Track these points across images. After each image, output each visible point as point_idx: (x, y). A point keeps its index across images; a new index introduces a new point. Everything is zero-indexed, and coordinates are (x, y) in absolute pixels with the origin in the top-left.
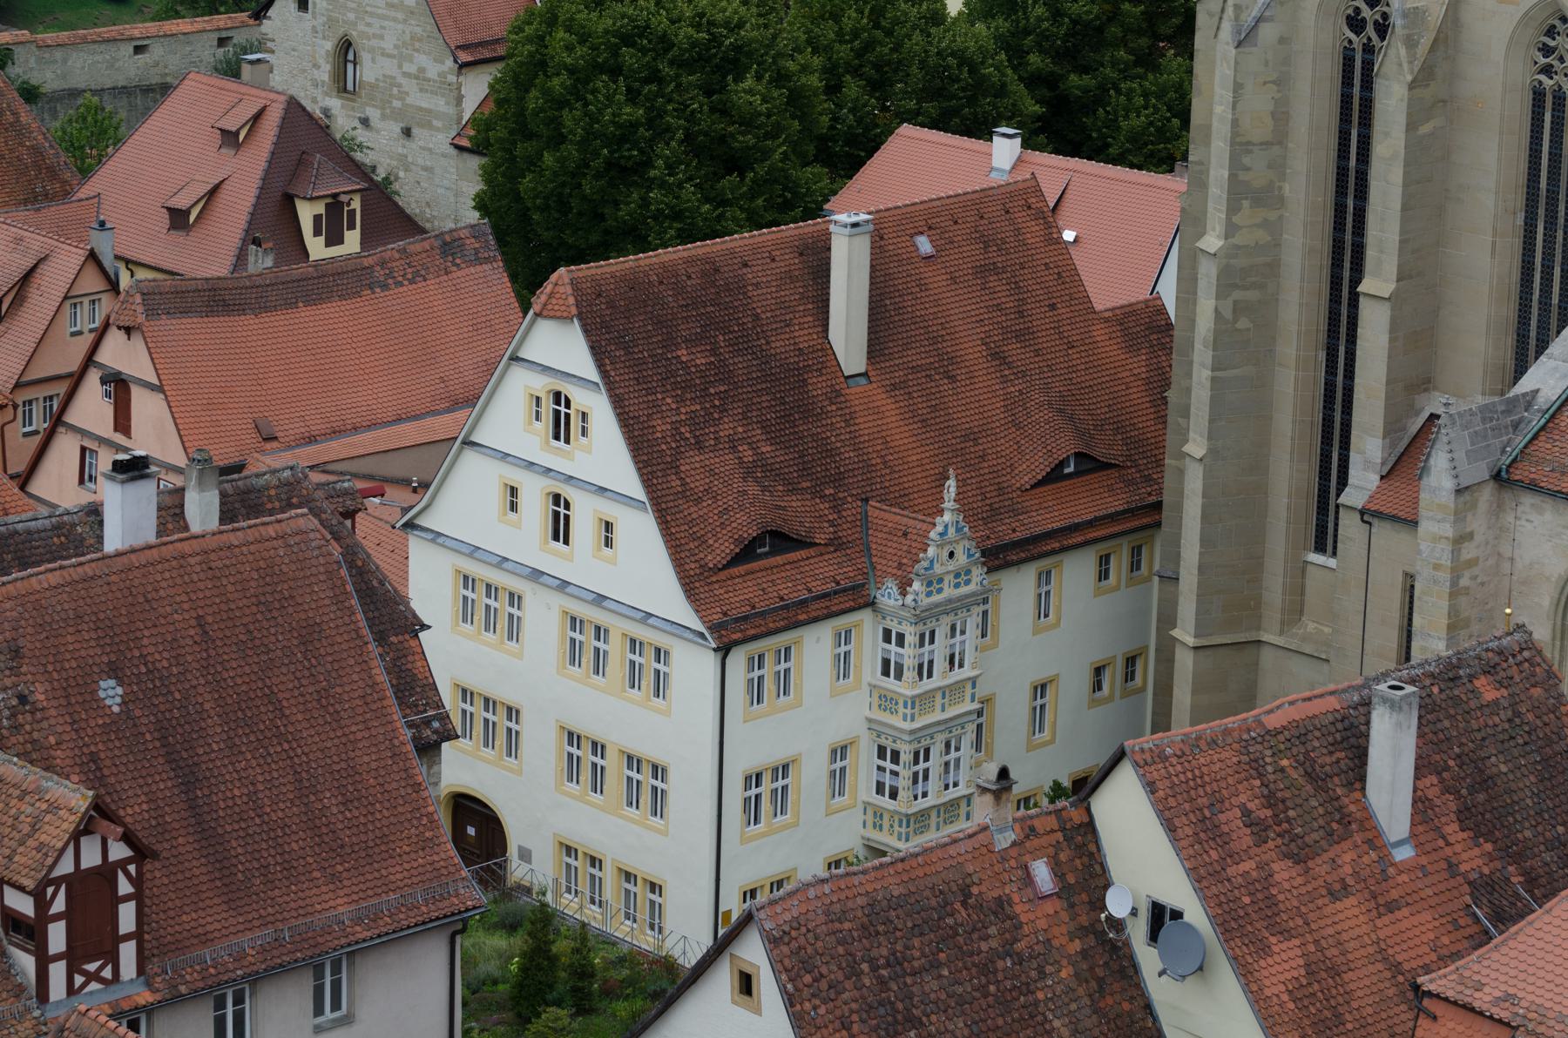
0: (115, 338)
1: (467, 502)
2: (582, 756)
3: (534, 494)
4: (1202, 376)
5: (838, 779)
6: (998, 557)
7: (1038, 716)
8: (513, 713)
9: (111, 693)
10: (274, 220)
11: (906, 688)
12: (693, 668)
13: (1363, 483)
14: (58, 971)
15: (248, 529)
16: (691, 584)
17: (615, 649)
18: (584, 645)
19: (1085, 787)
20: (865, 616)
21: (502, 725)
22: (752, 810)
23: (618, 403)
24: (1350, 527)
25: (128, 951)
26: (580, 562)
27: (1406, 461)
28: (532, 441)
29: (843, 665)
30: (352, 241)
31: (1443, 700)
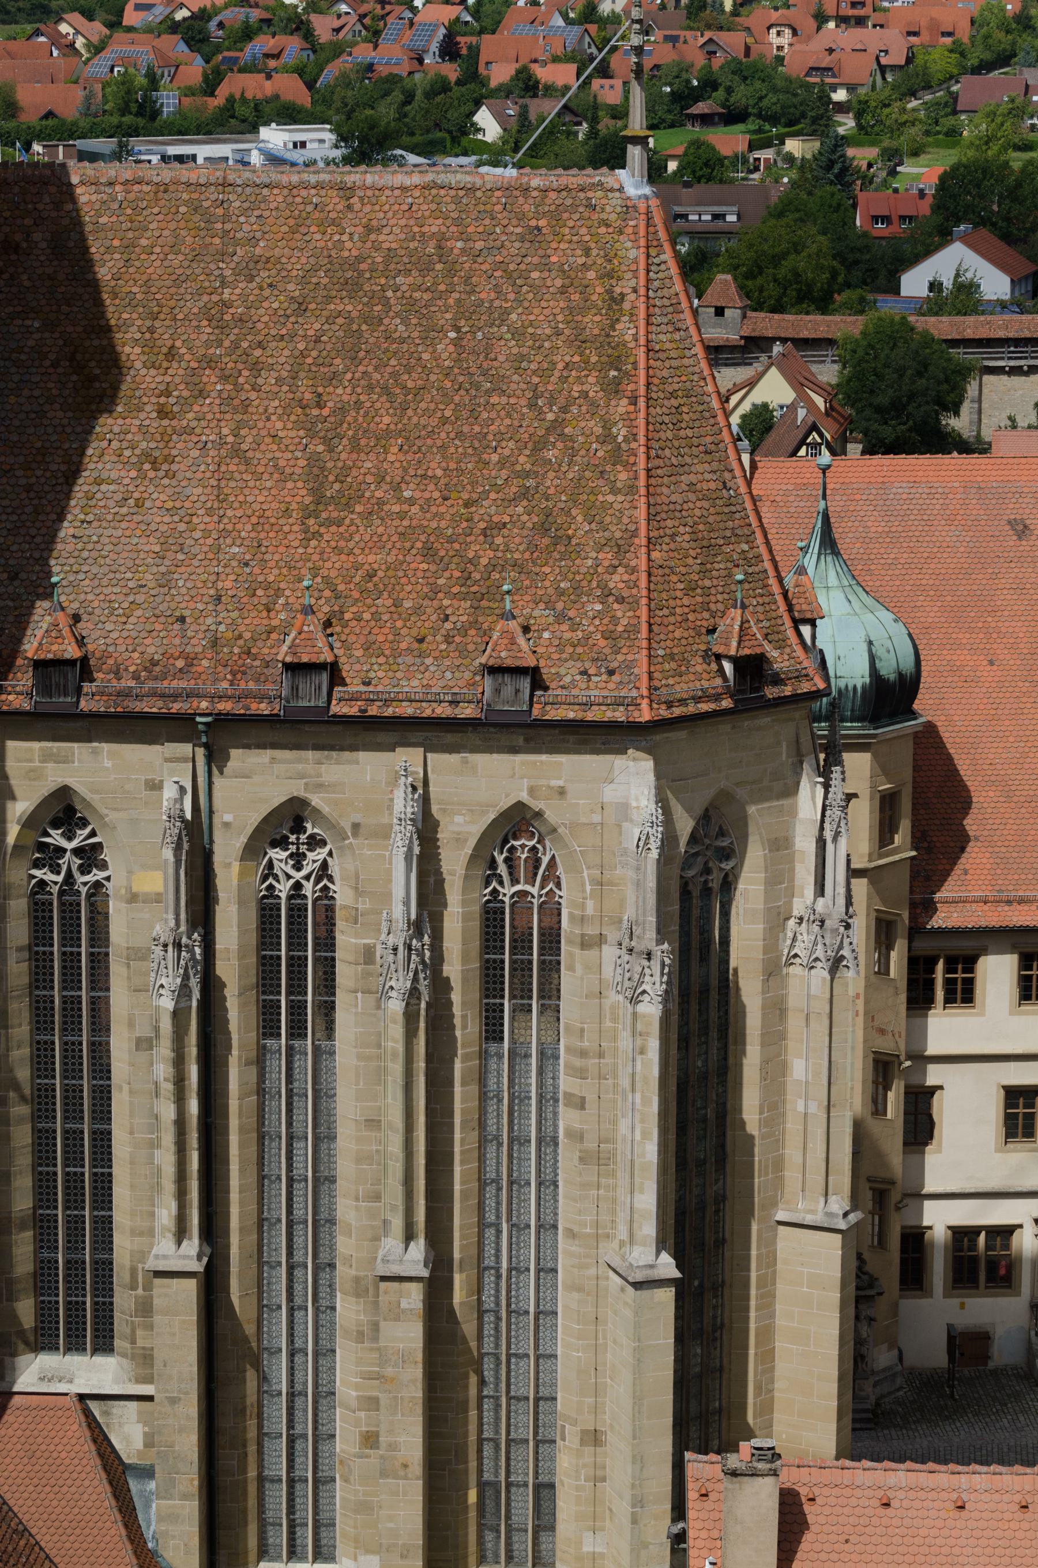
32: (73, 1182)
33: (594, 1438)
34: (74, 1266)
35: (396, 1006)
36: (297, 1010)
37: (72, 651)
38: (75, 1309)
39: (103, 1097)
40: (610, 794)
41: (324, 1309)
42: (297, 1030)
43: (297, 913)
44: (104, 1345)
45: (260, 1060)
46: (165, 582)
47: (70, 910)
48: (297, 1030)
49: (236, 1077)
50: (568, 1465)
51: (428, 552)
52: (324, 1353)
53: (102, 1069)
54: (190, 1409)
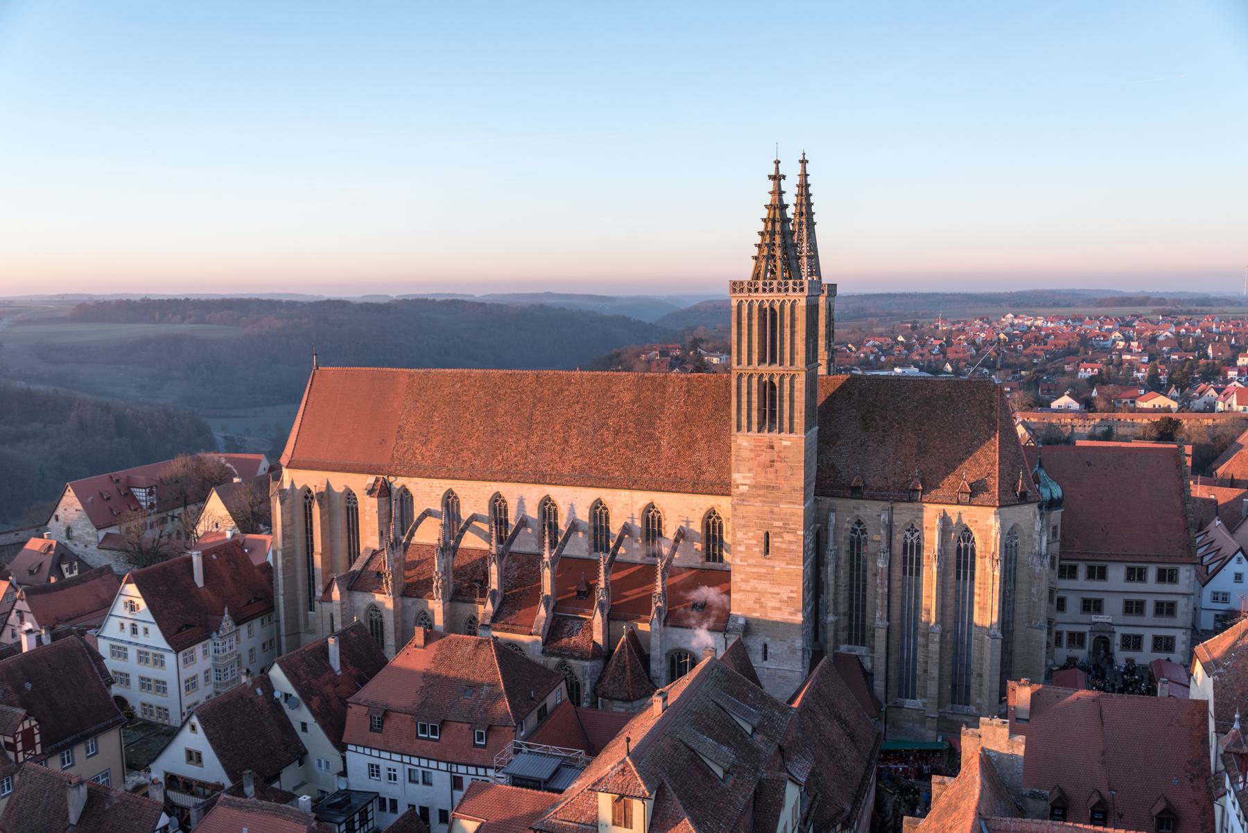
0: (19, 602)
1: (112, 628)
2: (145, 683)
3: (127, 624)
4: (280, 576)
5: (207, 679)
6: (238, 623)
7: (251, 657)
8: (127, 675)
9: (28, 686)
10: (56, 568)
11: (221, 655)
12: (170, 658)
13: (319, 594)
14: (20, 755)
15: (59, 642)
16: (168, 639)
17: (150, 656)
18: (143, 658)
19: (264, 671)
20: (209, 641)
21: (125, 679)
22: (187, 688)
23: (146, 601)
24: (317, 604)
25: (38, 748)
26: (141, 638)
27: (328, 589)
28: (126, 613)
29: (205, 653)
30: (76, 573)
31: (343, 638)
32: (857, 606)
33: (980, 675)
34: (857, 625)
35: (935, 569)
36: (911, 569)
37: (861, 484)
38: (857, 635)
39: (865, 586)
40: (988, 522)
41: (915, 640)
42: (911, 574)
43: (912, 547)
44: (863, 645)
45: (903, 580)
46: (883, 469)
47: (859, 543)
48: (911, 574)
49: (896, 584)
50: (974, 680)
51: (945, 465)
52: (915, 649)
53: (865, 581)
54: (883, 661)
